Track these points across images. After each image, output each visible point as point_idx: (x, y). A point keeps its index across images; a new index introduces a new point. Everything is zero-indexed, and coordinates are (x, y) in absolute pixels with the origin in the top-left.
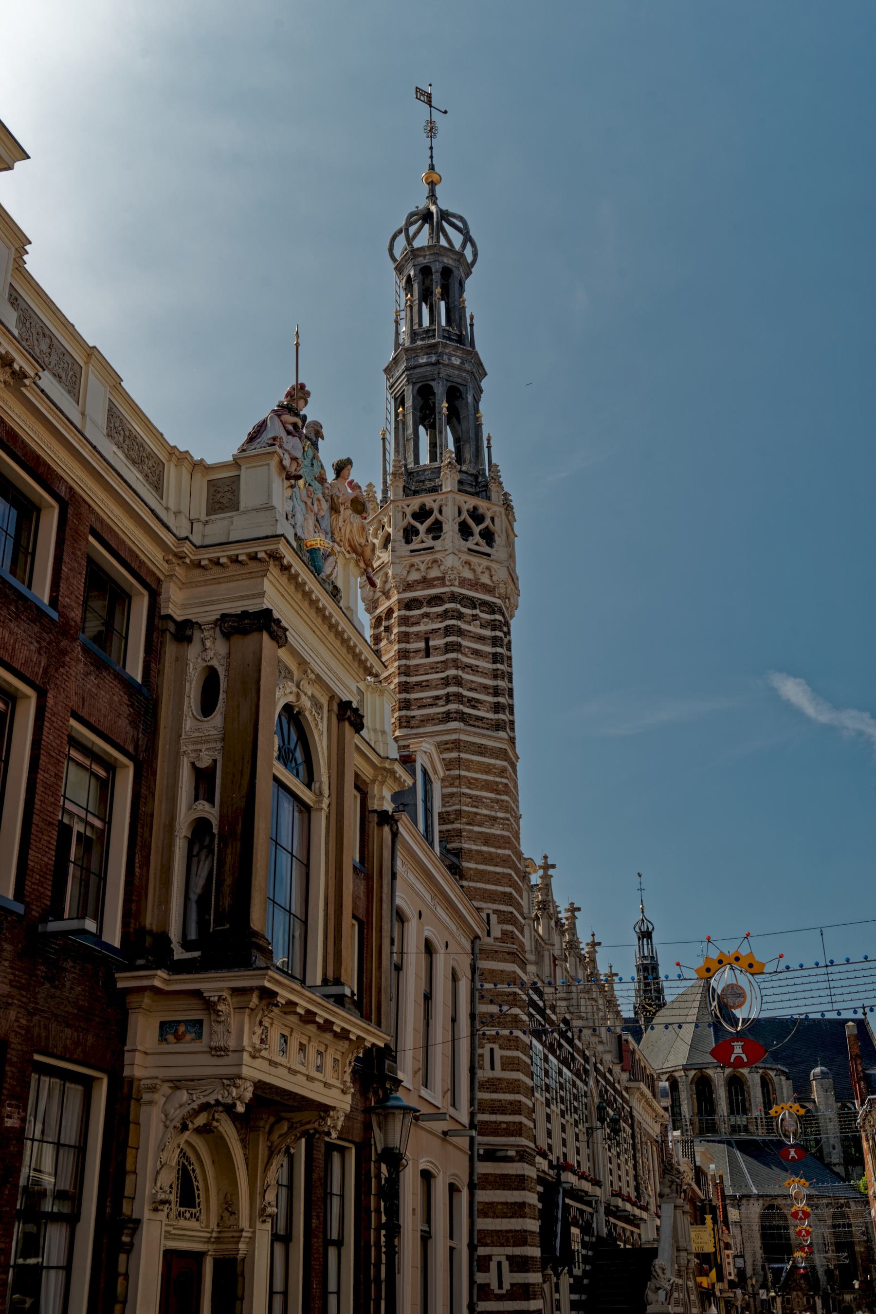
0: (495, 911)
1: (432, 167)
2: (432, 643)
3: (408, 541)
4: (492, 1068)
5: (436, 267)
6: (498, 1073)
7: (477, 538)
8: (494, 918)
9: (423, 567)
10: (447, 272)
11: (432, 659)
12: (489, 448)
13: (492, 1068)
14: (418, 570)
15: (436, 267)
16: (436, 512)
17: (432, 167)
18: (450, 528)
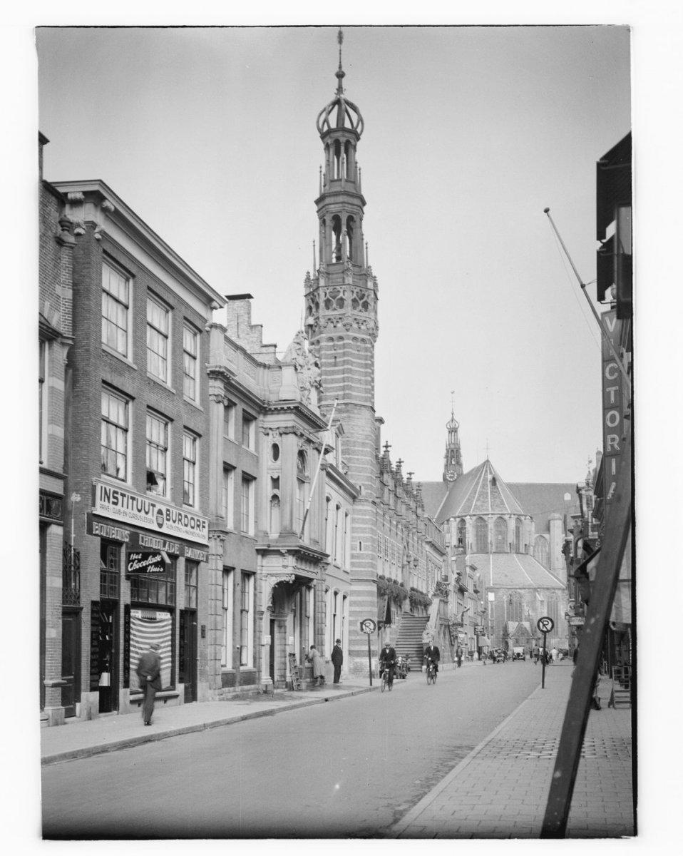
0: (363, 485)
1: (340, 67)
2: (338, 360)
3: (327, 308)
4: (360, 550)
5: (343, 140)
6: (362, 552)
7: (360, 307)
8: (362, 488)
9: (335, 321)
10: (348, 143)
11: (336, 368)
12: (367, 248)
13: (360, 550)
14: (332, 322)
15: (343, 140)
16: (341, 295)
17: (340, 67)
18: (348, 302)
